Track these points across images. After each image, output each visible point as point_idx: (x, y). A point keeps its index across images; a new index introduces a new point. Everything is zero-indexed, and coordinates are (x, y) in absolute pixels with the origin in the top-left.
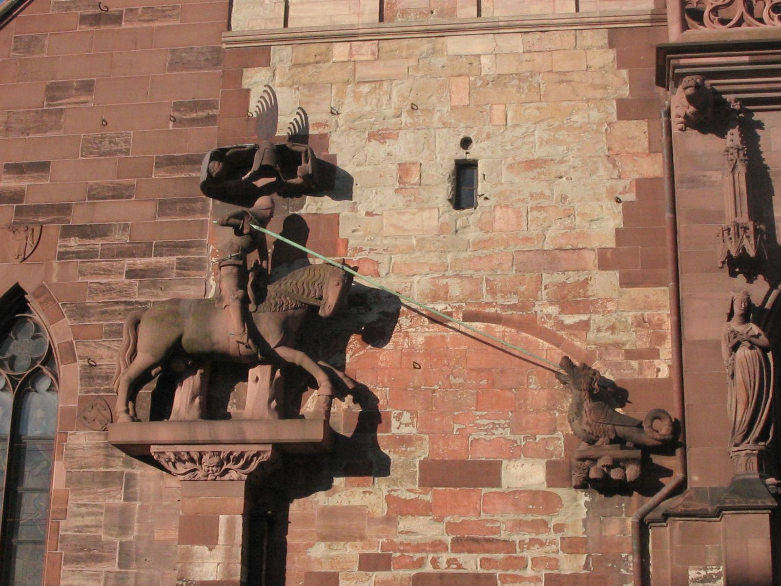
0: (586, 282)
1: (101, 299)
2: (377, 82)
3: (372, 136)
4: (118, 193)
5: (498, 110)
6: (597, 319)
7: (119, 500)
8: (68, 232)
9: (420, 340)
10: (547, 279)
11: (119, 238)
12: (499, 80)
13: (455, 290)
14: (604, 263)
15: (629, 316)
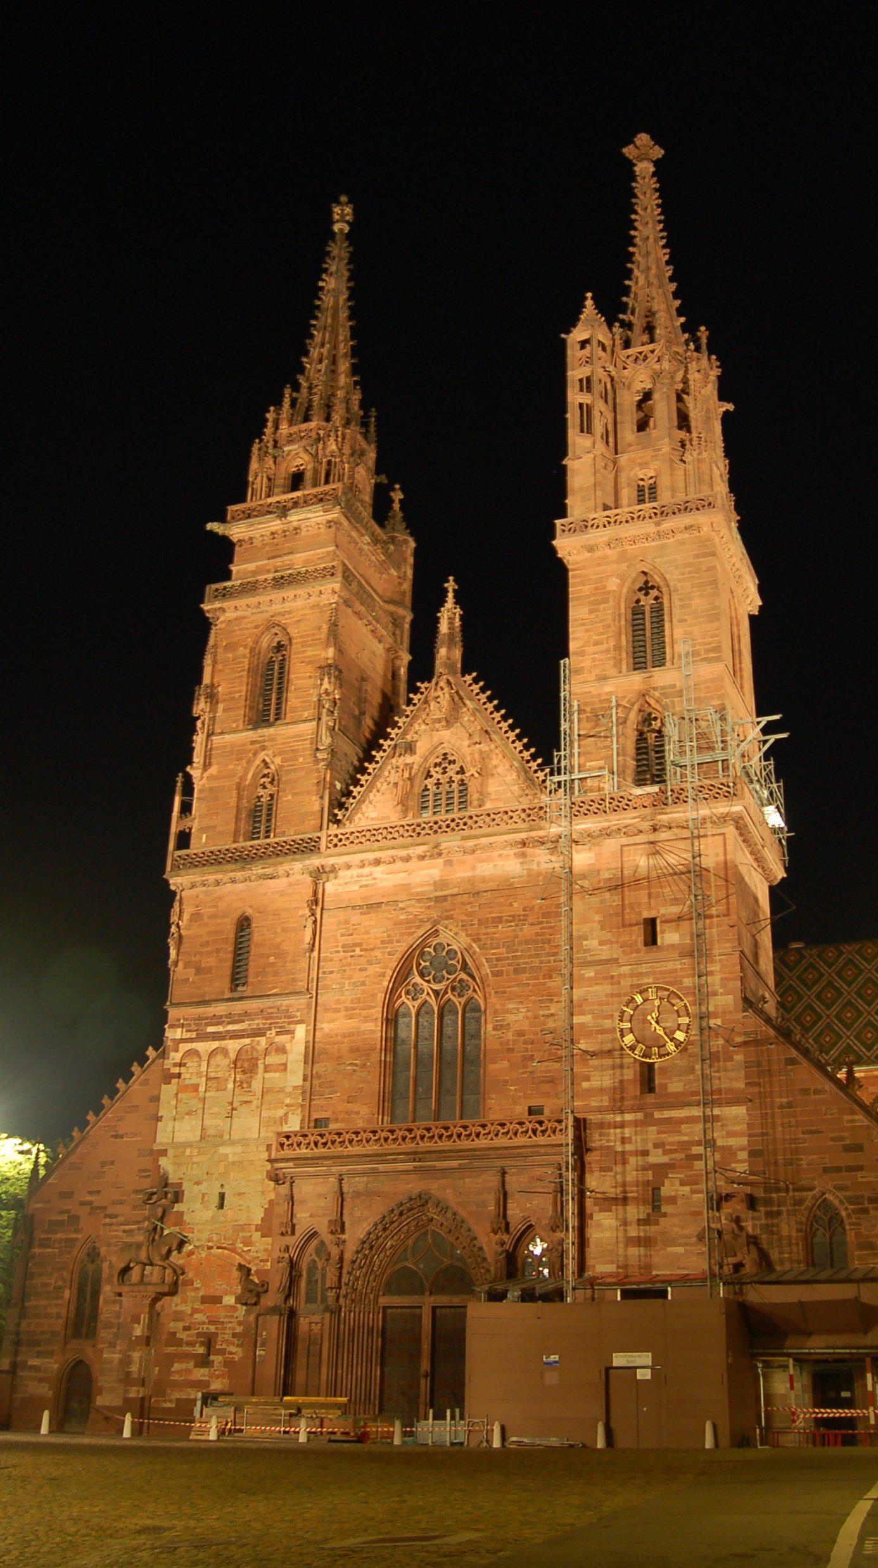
0: (251, 1236)
1: (115, 1240)
2: (198, 1163)
3: (195, 1183)
4: (121, 1203)
5: (232, 1174)
6: (253, 1248)
7: (117, 1308)
8: (106, 1216)
9: (204, 1255)
10: (241, 1234)
11: (121, 1219)
12: (234, 1163)
13: (215, 1238)
14: (256, 1231)
15: (262, 1248)
